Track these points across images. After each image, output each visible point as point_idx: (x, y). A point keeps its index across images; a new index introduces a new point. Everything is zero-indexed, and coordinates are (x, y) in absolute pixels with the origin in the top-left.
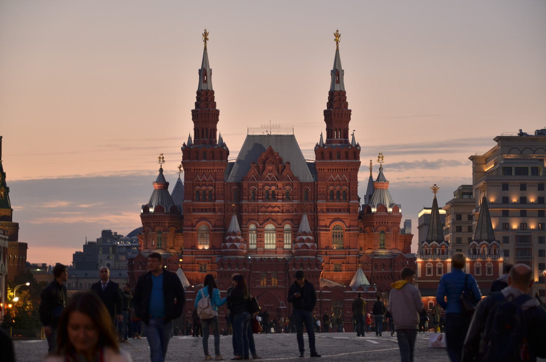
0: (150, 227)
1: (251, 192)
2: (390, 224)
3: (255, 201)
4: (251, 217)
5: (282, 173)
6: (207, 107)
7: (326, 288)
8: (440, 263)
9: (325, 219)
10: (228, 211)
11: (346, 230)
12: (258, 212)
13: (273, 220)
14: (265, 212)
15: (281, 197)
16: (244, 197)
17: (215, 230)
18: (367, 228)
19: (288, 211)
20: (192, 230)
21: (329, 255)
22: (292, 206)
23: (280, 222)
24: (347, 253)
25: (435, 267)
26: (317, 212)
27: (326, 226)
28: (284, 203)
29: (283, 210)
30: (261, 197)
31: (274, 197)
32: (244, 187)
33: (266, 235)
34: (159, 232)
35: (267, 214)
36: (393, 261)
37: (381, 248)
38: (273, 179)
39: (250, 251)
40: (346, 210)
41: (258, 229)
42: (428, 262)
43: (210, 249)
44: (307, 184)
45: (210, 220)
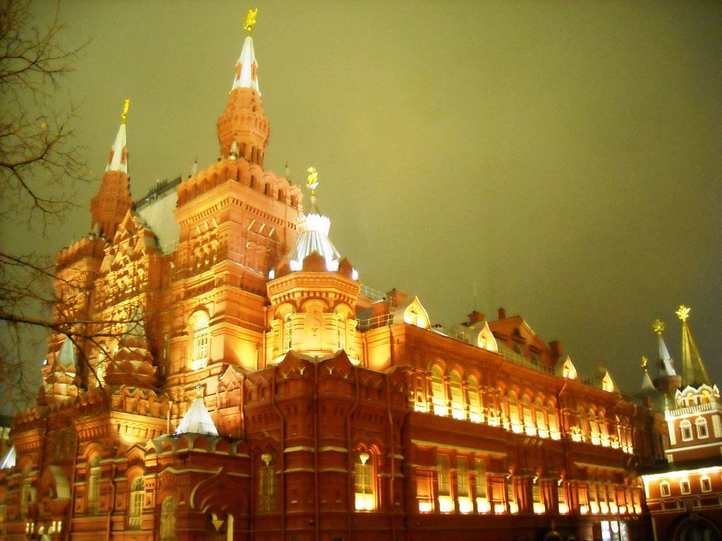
8: (701, 418)
11: (211, 324)
25: (694, 426)
42: (682, 420)
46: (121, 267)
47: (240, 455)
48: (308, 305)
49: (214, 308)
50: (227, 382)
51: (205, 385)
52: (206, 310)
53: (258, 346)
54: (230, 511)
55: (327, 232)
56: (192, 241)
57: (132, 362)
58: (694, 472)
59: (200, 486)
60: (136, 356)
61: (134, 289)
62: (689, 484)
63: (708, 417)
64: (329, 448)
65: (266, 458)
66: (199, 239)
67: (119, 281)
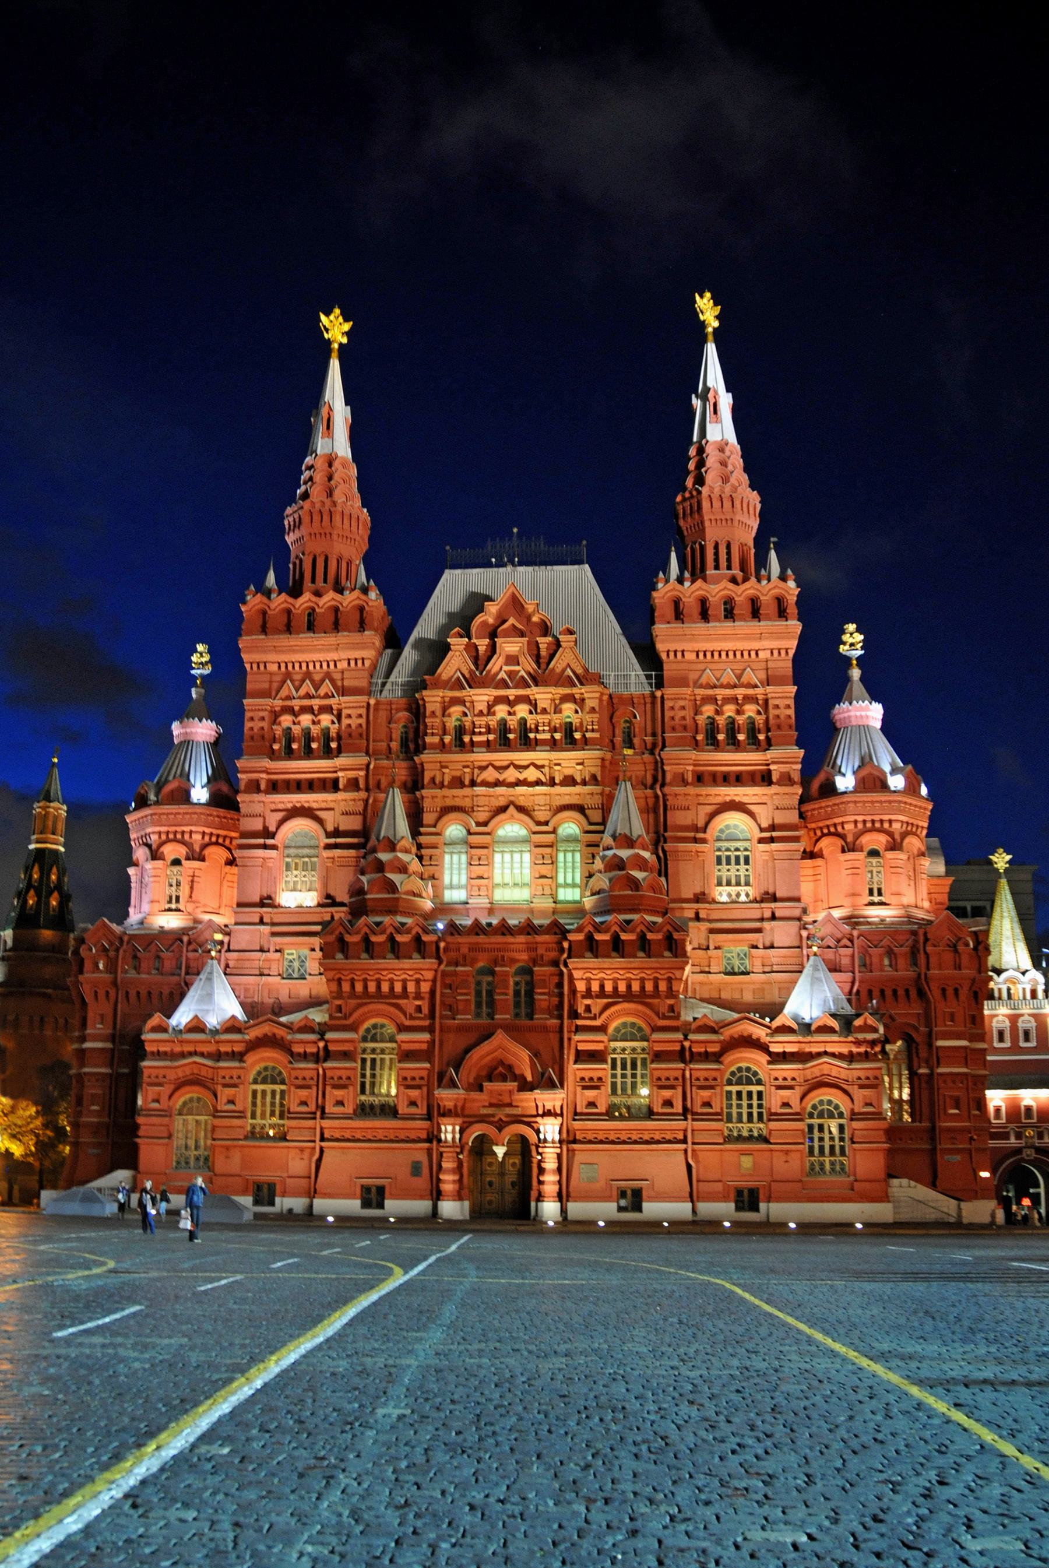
0: (149, 846)
1: (452, 723)
2: (896, 826)
3: (462, 752)
4: (449, 802)
5: (548, 664)
6: (330, 493)
9: (690, 804)
10: (378, 786)
11: (761, 841)
12: (473, 783)
13: (521, 809)
14: (497, 783)
15: (547, 736)
16: (428, 739)
17: (336, 846)
18: (825, 844)
19: (569, 781)
20: (265, 847)
21: (710, 921)
22: (582, 764)
23: (541, 816)
24: (768, 914)
26: (663, 785)
27: (696, 829)
28: (555, 755)
29: (552, 779)
30: (483, 738)
31: (526, 740)
32: (430, 708)
33: (497, 857)
34: (176, 862)
36: (921, 939)
38: (523, 684)
39: (442, 909)
40: (758, 778)
41: (473, 839)
43: (319, 905)
44: (631, 701)
45: (321, 814)
62: (1003, 1109)
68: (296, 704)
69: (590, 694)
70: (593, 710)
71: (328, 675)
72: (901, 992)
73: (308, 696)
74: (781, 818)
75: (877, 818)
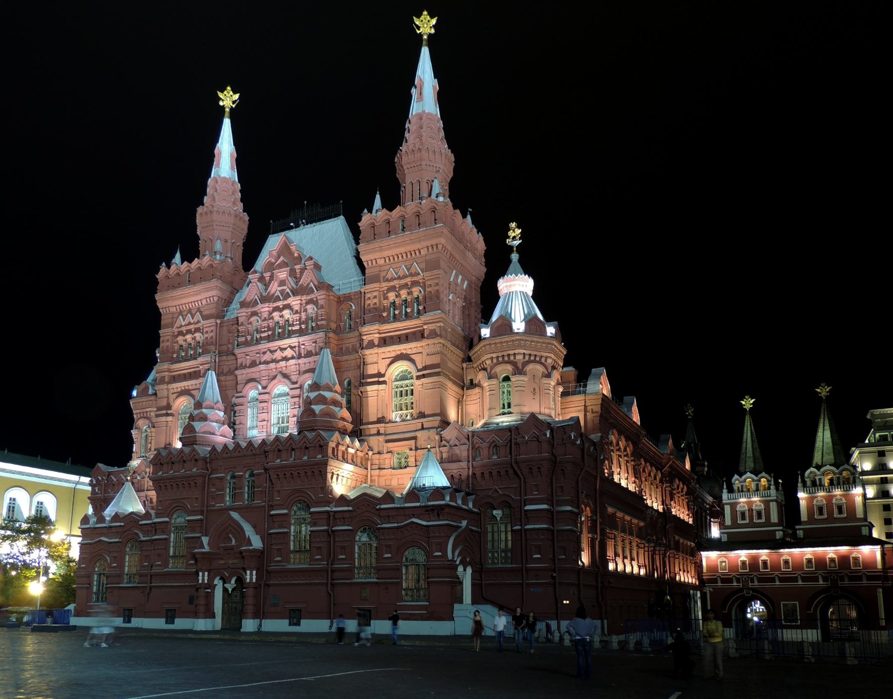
2: (518, 357)
7: (343, 499)
9: (376, 359)
11: (418, 378)
15: (297, 327)
19: (309, 354)
21: (386, 435)
22: (316, 342)
25: (751, 510)
28: (302, 339)
29: (300, 354)
30: (266, 334)
35: (272, 365)
37: (504, 414)
46: (278, 299)
47: (475, 510)
48: (530, 367)
49: (420, 361)
50: (448, 438)
51: (415, 438)
52: (413, 361)
53: (460, 402)
54: (470, 564)
55: (530, 294)
56: (385, 285)
57: (313, 407)
58: (754, 552)
59: (455, 539)
60: (335, 403)
61: (303, 326)
63: (767, 503)
64: (569, 508)
65: (497, 513)
66: (396, 283)
67: (276, 315)
68: (184, 329)
69: (320, 295)
70: (322, 307)
71: (199, 310)
72: (503, 472)
73: (190, 324)
74: (429, 361)
75: (505, 353)
